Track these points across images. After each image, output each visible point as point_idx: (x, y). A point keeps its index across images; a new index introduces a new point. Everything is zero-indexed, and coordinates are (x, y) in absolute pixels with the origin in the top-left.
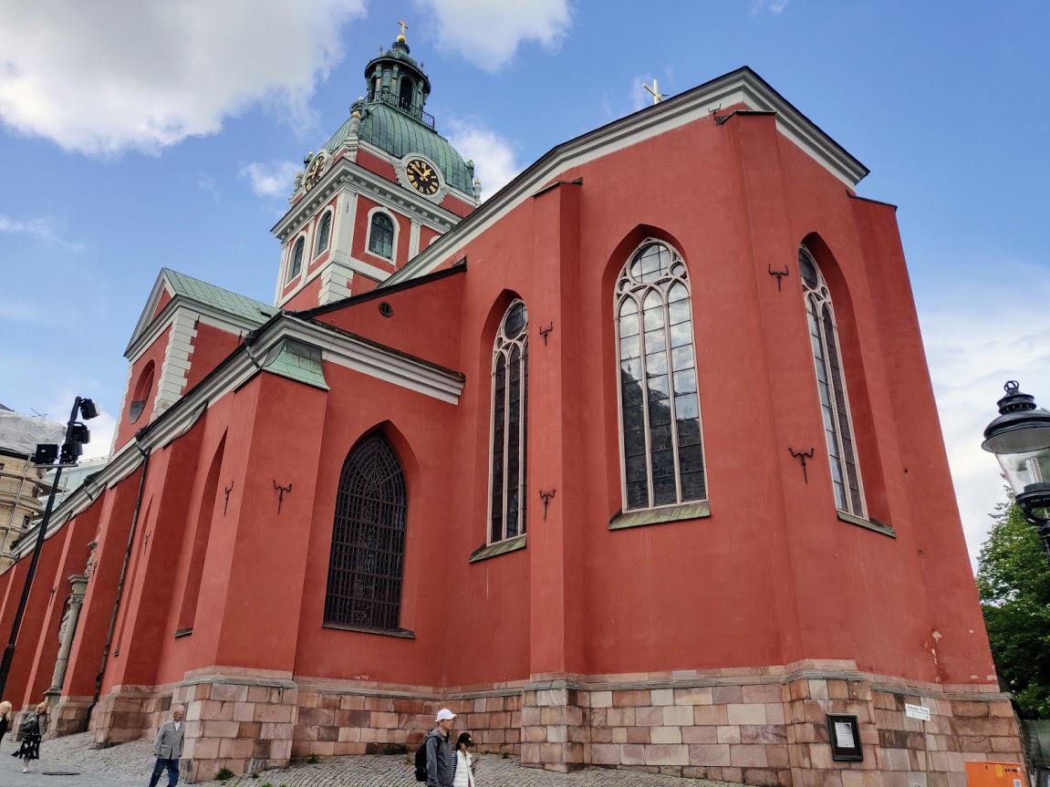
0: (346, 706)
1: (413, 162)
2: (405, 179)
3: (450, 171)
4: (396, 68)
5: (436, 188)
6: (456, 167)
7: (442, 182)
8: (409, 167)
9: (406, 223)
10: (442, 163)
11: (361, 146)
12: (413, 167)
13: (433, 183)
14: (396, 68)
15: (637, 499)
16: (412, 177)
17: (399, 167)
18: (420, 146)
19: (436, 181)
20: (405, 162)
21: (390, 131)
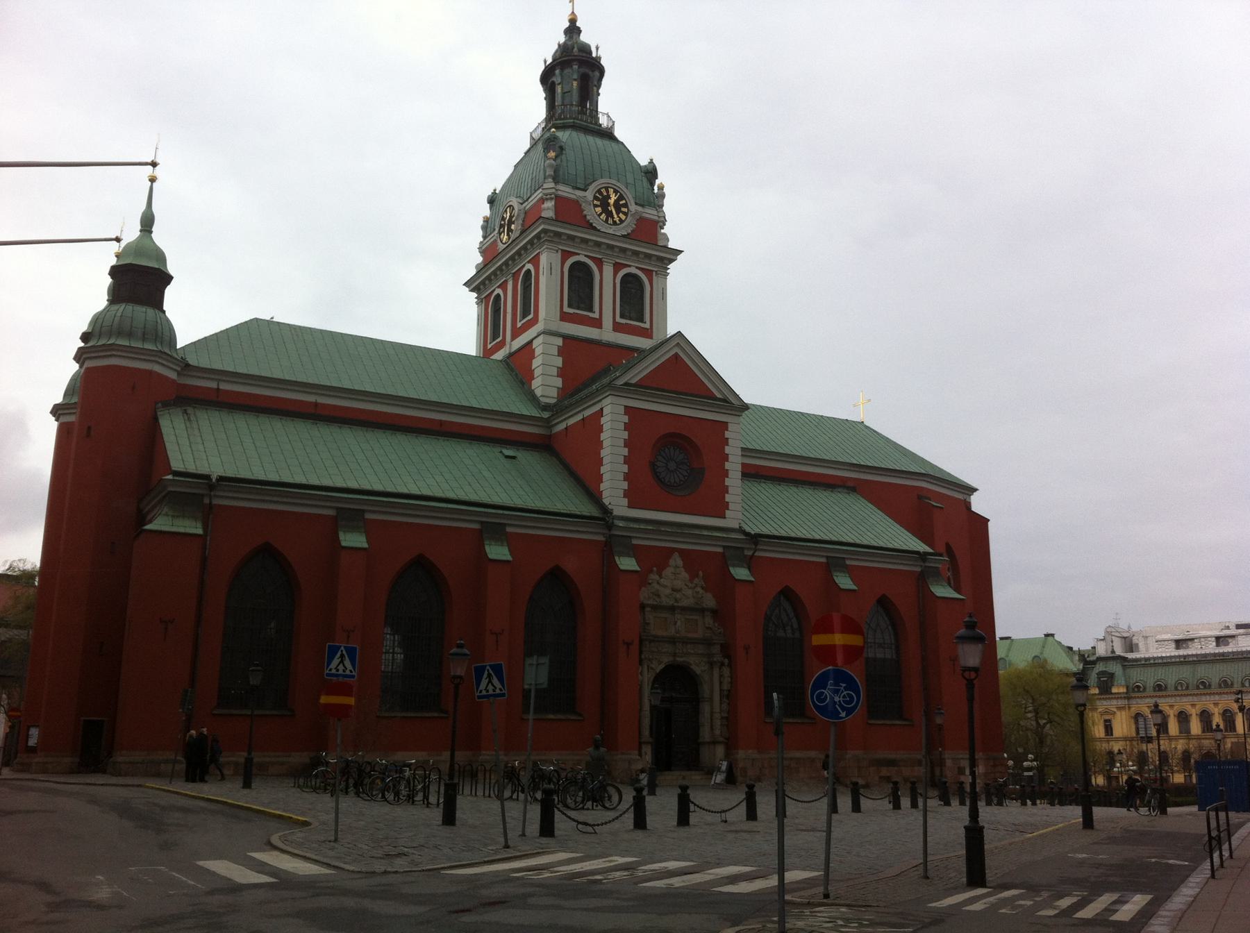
2: (593, 213)
4: (576, 67)
13: (623, 209)
16: (599, 210)
17: (586, 202)
19: (626, 205)
20: (589, 195)
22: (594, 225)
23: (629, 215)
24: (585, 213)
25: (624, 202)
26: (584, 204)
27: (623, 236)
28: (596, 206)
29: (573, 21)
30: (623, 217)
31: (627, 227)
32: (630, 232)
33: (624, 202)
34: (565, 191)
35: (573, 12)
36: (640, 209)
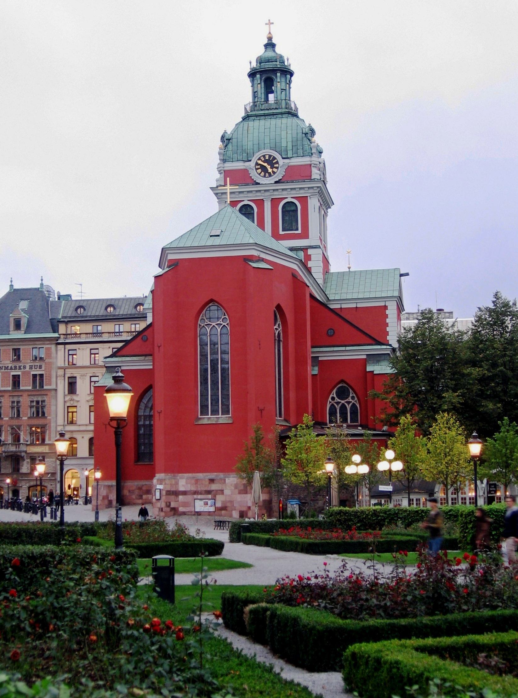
0: (144, 488)
1: (259, 159)
2: (255, 175)
3: (290, 147)
4: (258, 76)
5: (277, 168)
6: (295, 139)
7: (281, 161)
8: (257, 164)
9: (260, 203)
10: (284, 144)
11: (225, 169)
12: (260, 162)
14: (258, 76)
15: (204, 411)
16: (259, 171)
18: (267, 141)
19: (277, 163)
20: (252, 164)
21: (245, 143)
22: (257, 181)
23: (279, 168)
24: (251, 175)
25: (276, 161)
26: (250, 170)
27: (276, 182)
28: (257, 169)
29: (270, 39)
30: (275, 170)
31: (280, 174)
32: (281, 178)
33: (276, 161)
34: (239, 165)
35: (270, 33)
36: (287, 161)
